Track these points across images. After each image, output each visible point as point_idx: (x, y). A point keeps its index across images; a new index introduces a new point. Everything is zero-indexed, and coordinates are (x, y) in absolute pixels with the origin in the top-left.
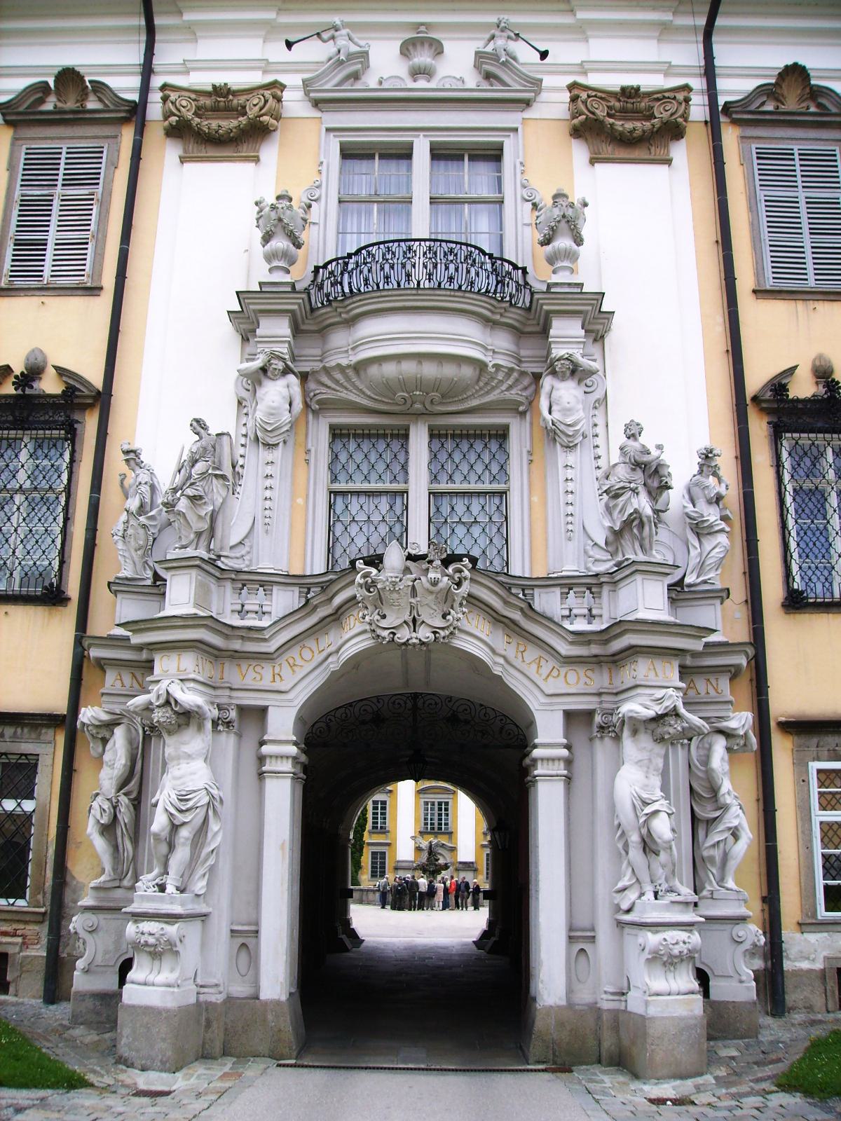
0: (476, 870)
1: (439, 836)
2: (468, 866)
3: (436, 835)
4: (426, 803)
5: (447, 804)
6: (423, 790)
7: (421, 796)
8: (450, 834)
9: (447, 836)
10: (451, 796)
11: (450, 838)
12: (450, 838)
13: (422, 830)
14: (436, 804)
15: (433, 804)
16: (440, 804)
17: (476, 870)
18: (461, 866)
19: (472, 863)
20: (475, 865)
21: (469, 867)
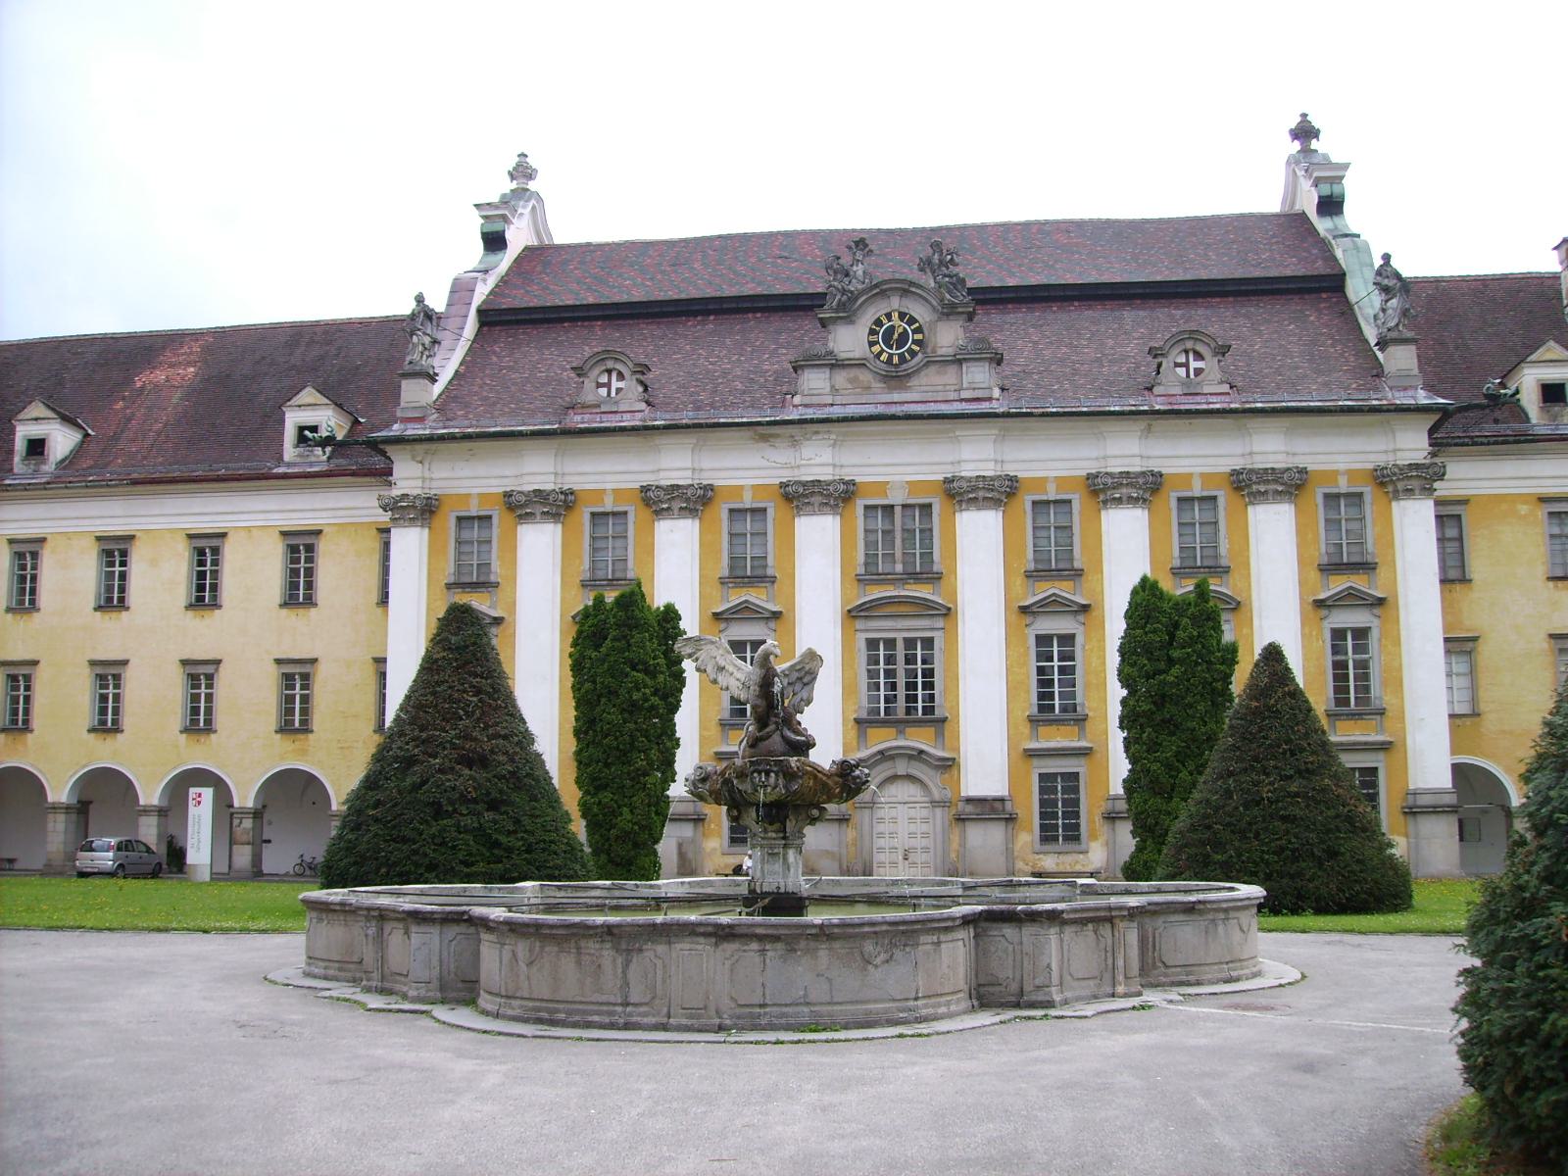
0: (1010, 819)
1: (909, 730)
2: (989, 809)
3: (900, 725)
4: (872, 644)
5: (928, 643)
6: (861, 608)
7: (860, 624)
8: (936, 721)
9: (930, 731)
10: (939, 623)
11: (940, 735)
12: (940, 735)
13: (864, 715)
14: (900, 645)
15: (890, 644)
16: (910, 643)
17: (1010, 819)
18: (969, 808)
19: (1002, 800)
20: (1008, 805)
21: (993, 810)
